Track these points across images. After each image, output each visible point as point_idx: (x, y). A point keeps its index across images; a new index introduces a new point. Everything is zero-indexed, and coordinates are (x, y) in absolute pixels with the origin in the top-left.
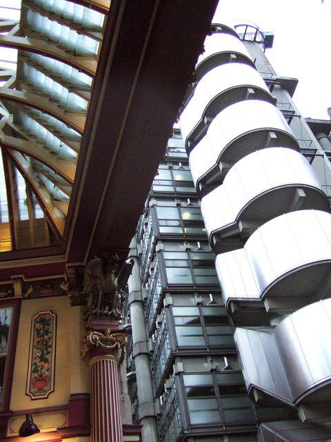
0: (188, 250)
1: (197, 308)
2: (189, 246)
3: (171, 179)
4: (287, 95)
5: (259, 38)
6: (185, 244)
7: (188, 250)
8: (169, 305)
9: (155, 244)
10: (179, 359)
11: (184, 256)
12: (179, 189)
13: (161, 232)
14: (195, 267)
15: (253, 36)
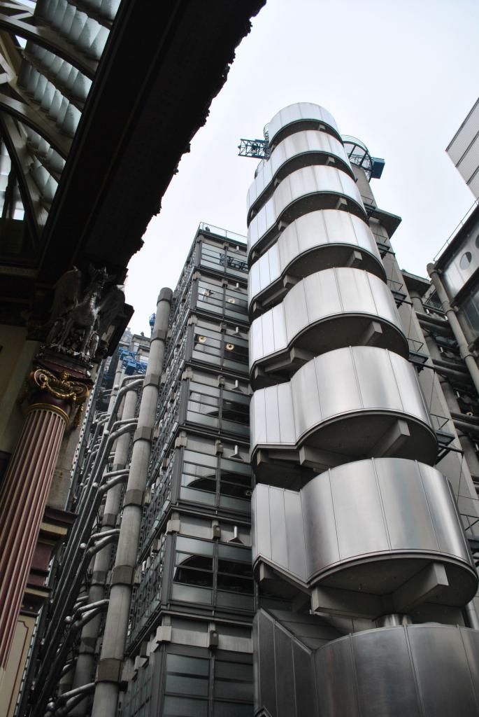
0: (221, 386)
1: (216, 458)
4: (385, 234)
5: (366, 164)
8: (181, 446)
9: (183, 370)
11: (216, 392)
12: (228, 313)
13: (193, 357)
15: (360, 160)
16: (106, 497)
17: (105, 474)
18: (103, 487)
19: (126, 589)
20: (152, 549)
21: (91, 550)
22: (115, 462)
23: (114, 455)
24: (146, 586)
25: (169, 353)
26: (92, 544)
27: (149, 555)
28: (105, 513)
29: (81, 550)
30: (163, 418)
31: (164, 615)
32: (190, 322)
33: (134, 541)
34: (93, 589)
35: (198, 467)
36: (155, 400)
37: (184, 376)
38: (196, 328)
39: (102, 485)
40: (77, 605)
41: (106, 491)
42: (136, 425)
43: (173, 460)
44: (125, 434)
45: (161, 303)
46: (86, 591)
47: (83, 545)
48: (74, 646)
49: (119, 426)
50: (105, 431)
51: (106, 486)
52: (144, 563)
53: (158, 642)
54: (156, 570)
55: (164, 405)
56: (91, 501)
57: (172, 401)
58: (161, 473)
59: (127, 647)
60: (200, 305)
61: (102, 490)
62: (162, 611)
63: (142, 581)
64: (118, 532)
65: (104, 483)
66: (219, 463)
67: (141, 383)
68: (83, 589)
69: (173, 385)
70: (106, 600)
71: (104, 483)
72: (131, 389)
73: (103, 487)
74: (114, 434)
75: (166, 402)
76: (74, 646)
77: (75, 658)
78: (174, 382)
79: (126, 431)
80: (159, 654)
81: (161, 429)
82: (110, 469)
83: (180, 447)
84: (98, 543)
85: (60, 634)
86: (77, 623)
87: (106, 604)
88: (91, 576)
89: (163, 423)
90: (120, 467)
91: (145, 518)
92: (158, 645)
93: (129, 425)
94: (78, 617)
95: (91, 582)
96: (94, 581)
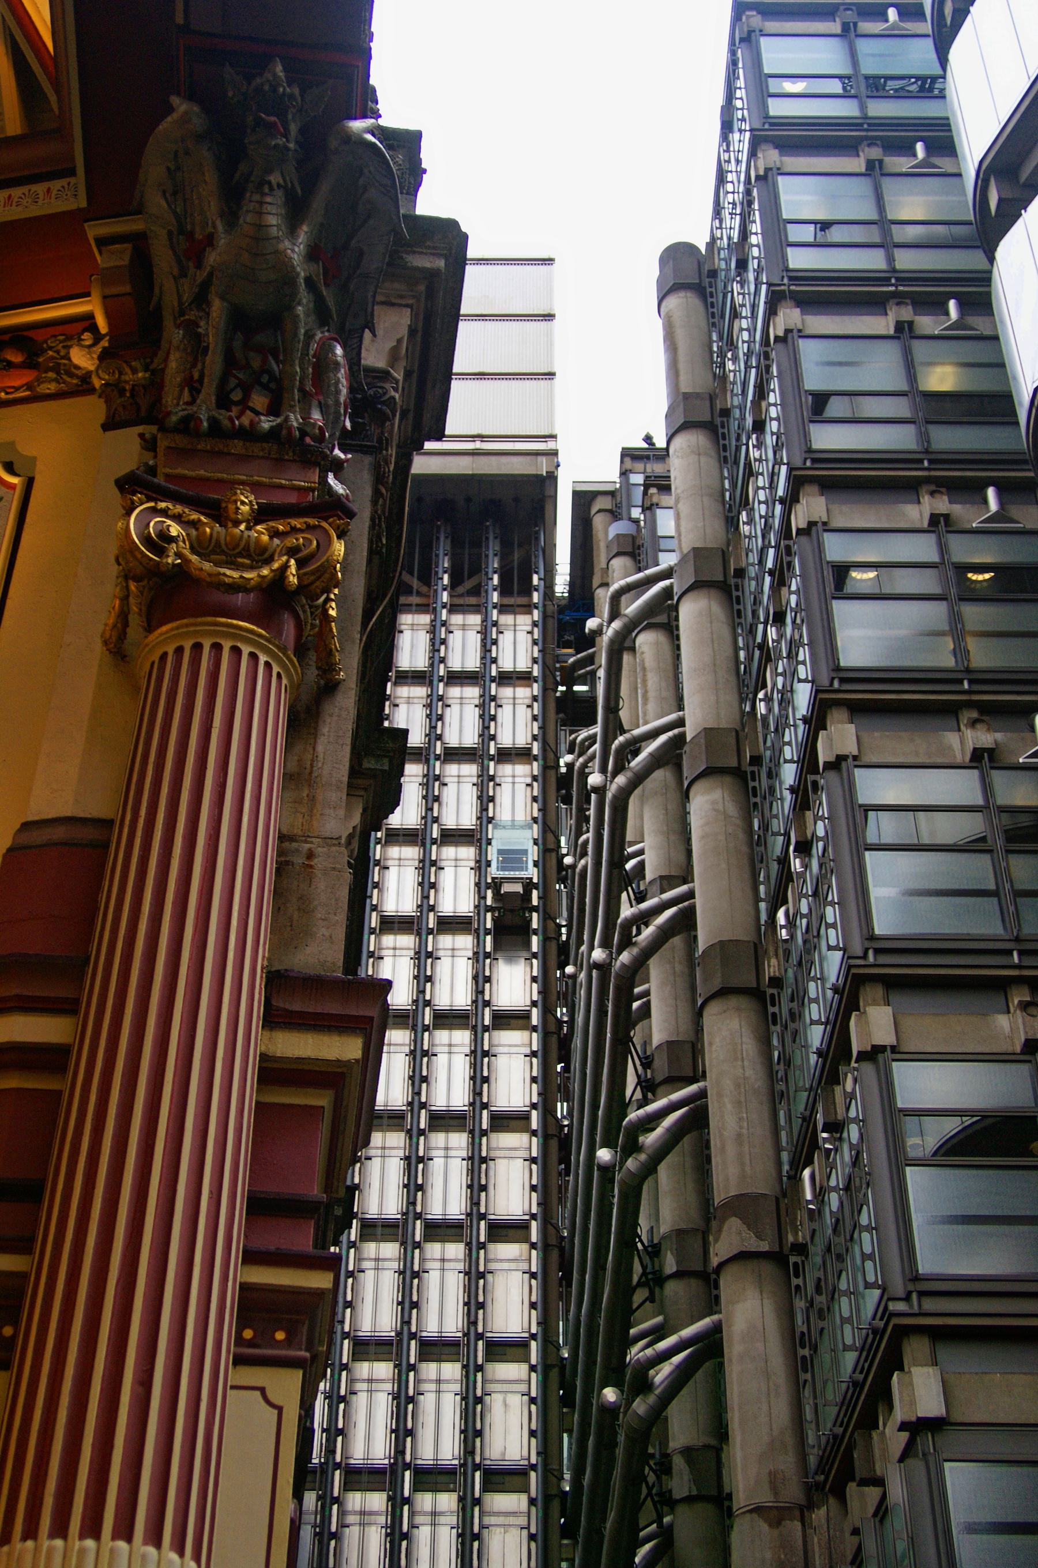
0: (938, 523)
1: (976, 772)
2: (942, 505)
3: (874, 216)
6: (926, 499)
7: (938, 523)
8: (841, 759)
9: (790, 501)
10: (879, 991)
11: (924, 548)
12: (907, 261)
14: (970, 595)
16: (647, 993)
17: (626, 911)
18: (625, 957)
19: (768, 1268)
20: (820, 1126)
21: (631, 1164)
22: (649, 874)
23: (641, 852)
24: (829, 1249)
25: (736, 462)
26: (632, 1147)
27: (814, 1145)
28: (656, 1040)
29: (607, 1170)
30: (764, 686)
31: (903, 1332)
32: (778, 328)
33: (758, 1111)
34: (672, 1288)
35: (921, 815)
36: (726, 632)
37: (799, 520)
38: (802, 343)
39: (619, 952)
40: (634, 1350)
41: (638, 968)
42: (683, 735)
43: (824, 811)
44: (659, 775)
45: (673, 302)
46: (651, 1299)
47: (604, 1155)
48: (651, 1478)
49: (633, 747)
50: (595, 779)
51: (635, 951)
52: (806, 1173)
53: (903, 1426)
54: (847, 1188)
55: (759, 639)
56: (602, 1012)
57: (779, 619)
58: (796, 865)
59: (813, 1460)
60: (799, 260)
61: (623, 965)
62: (895, 1321)
63: (813, 1233)
64: (703, 1094)
65: (627, 942)
66: (987, 788)
67: (668, 592)
68: (639, 1296)
69: (770, 564)
70: (715, 1317)
71: (627, 942)
72: (646, 619)
73: (625, 957)
74: (621, 780)
75: (761, 627)
76: (651, 1478)
77: (667, 1520)
78: (771, 552)
79: (657, 761)
80: (916, 1465)
81: (765, 719)
82: (641, 898)
83: (837, 764)
84: (650, 1139)
85: (607, 1445)
86: (640, 1406)
87: (717, 1329)
88: (655, 1251)
89: (768, 699)
90: (666, 882)
91: (778, 1028)
92: (905, 1436)
93: (663, 738)
94: (641, 1384)
95: (661, 1270)
96: (670, 1264)
